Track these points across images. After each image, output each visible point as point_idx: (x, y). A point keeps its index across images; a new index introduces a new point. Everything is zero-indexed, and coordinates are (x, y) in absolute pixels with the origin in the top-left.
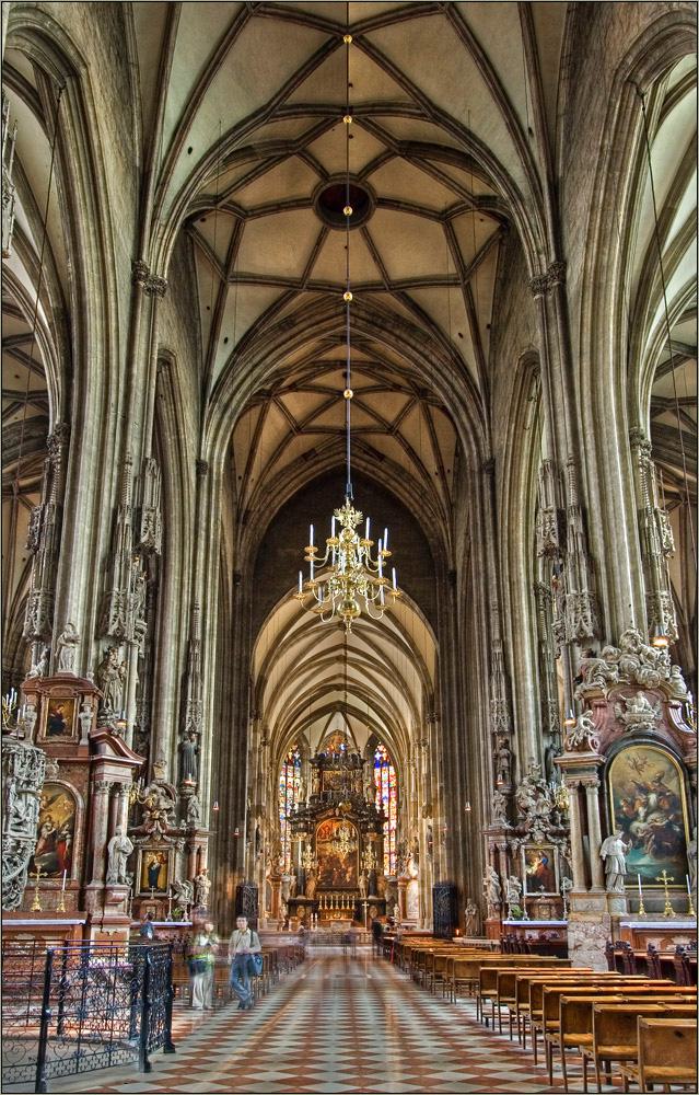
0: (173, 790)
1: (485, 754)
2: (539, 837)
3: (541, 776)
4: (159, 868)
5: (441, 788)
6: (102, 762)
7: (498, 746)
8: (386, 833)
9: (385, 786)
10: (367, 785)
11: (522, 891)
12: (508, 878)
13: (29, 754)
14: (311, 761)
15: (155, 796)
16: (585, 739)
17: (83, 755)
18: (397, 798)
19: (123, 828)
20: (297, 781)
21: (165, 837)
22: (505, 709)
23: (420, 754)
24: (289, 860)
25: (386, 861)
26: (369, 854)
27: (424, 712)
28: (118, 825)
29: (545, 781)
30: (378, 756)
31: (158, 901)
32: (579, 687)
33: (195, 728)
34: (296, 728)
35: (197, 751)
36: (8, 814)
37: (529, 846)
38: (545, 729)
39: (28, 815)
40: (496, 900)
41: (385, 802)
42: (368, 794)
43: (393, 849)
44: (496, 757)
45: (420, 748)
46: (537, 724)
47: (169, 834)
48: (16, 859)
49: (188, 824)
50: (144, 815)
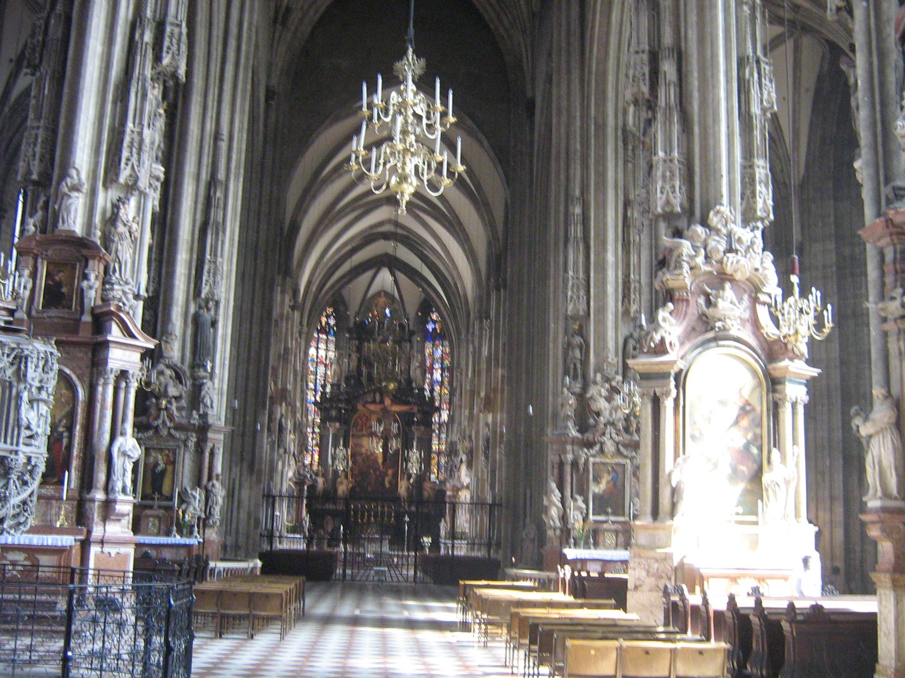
0: (184, 373)
1: (556, 339)
2: (610, 447)
3: (617, 373)
4: (164, 472)
5: (503, 376)
6: (106, 344)
7: (570, 331)
8: (435, 427)
9: (437, 366)
10: (415, 364)
11: (587, 514)
12: (572, 497)
13: (42, 355)
14: (350, 331)
15: (162, 378)
16: (662, 340)
17: (85, 334)
18: (451, 382)
19: (129, 427)
20: (332, 355)
21: (172, 431)
22: (581, 288)
23: (481, 329)
24: (316, 457)
25: (434, 462)
26: (415, 455)
27: (488, 279)
28: (123, 421)
29: (619, 378)
30: (430, 327)
31: (161, 512)
32: (660, 273)
33: (213, 294)
34: (332, 286)
35: (214, 324)
36: (19, 427)
37: (598, 460)
38: (626, 312)
39: (39, 426)
40: (558, 524)
41: (437, 388)
42: (415, 373)
43: (443, 447)
44: (568, 346)
45: (481, 322)
46: (616, 307)
47: (178, 427)
48: (27, 477)
49: (200, 415)
50: (148, 403)
